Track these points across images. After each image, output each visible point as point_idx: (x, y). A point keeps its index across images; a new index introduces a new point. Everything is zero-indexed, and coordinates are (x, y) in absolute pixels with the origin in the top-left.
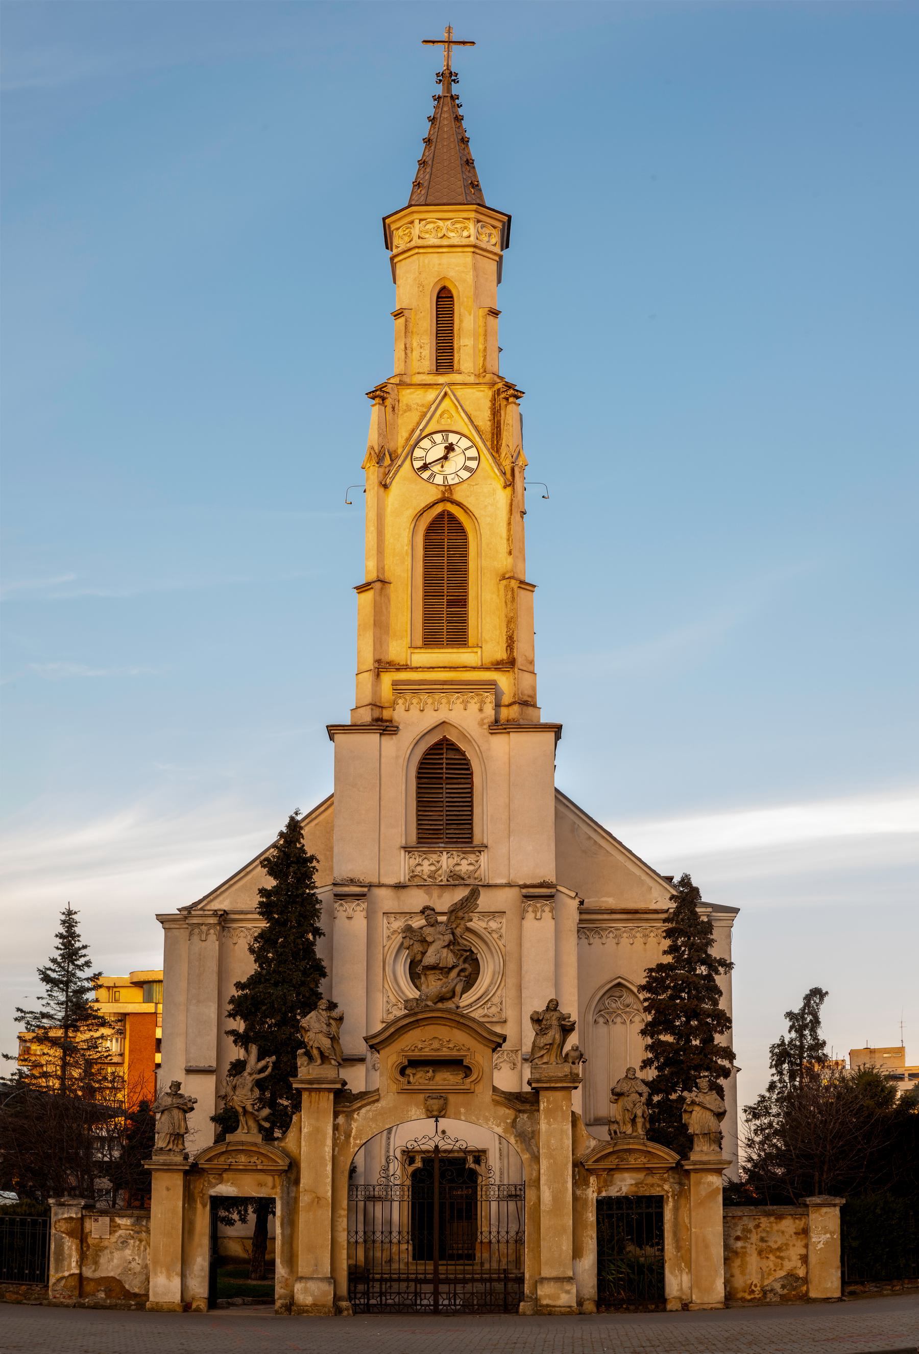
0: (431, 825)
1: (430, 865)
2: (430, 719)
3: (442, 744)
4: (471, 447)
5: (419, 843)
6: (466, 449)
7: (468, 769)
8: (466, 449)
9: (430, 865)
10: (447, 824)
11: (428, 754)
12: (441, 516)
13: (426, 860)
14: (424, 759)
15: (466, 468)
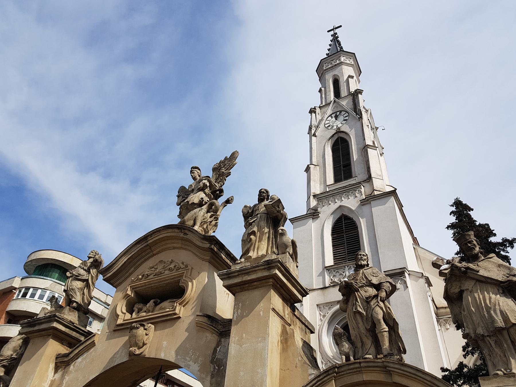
0: (340, 256)
1: (340, 275)
2: (333, 206)
3: (342, 218)
4: (346, 113)
5: (335, 264)
6: (344, 115)
7: (355, 226)
8: (344, 115)
9: (340, 275)
10: (348, 254)
11: (336, 224)
12: (337, 139)
13: (338, 273)
14: (334, 226)
15: (345, 120)
